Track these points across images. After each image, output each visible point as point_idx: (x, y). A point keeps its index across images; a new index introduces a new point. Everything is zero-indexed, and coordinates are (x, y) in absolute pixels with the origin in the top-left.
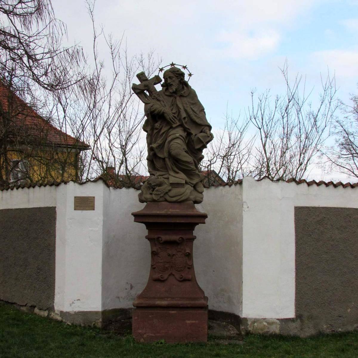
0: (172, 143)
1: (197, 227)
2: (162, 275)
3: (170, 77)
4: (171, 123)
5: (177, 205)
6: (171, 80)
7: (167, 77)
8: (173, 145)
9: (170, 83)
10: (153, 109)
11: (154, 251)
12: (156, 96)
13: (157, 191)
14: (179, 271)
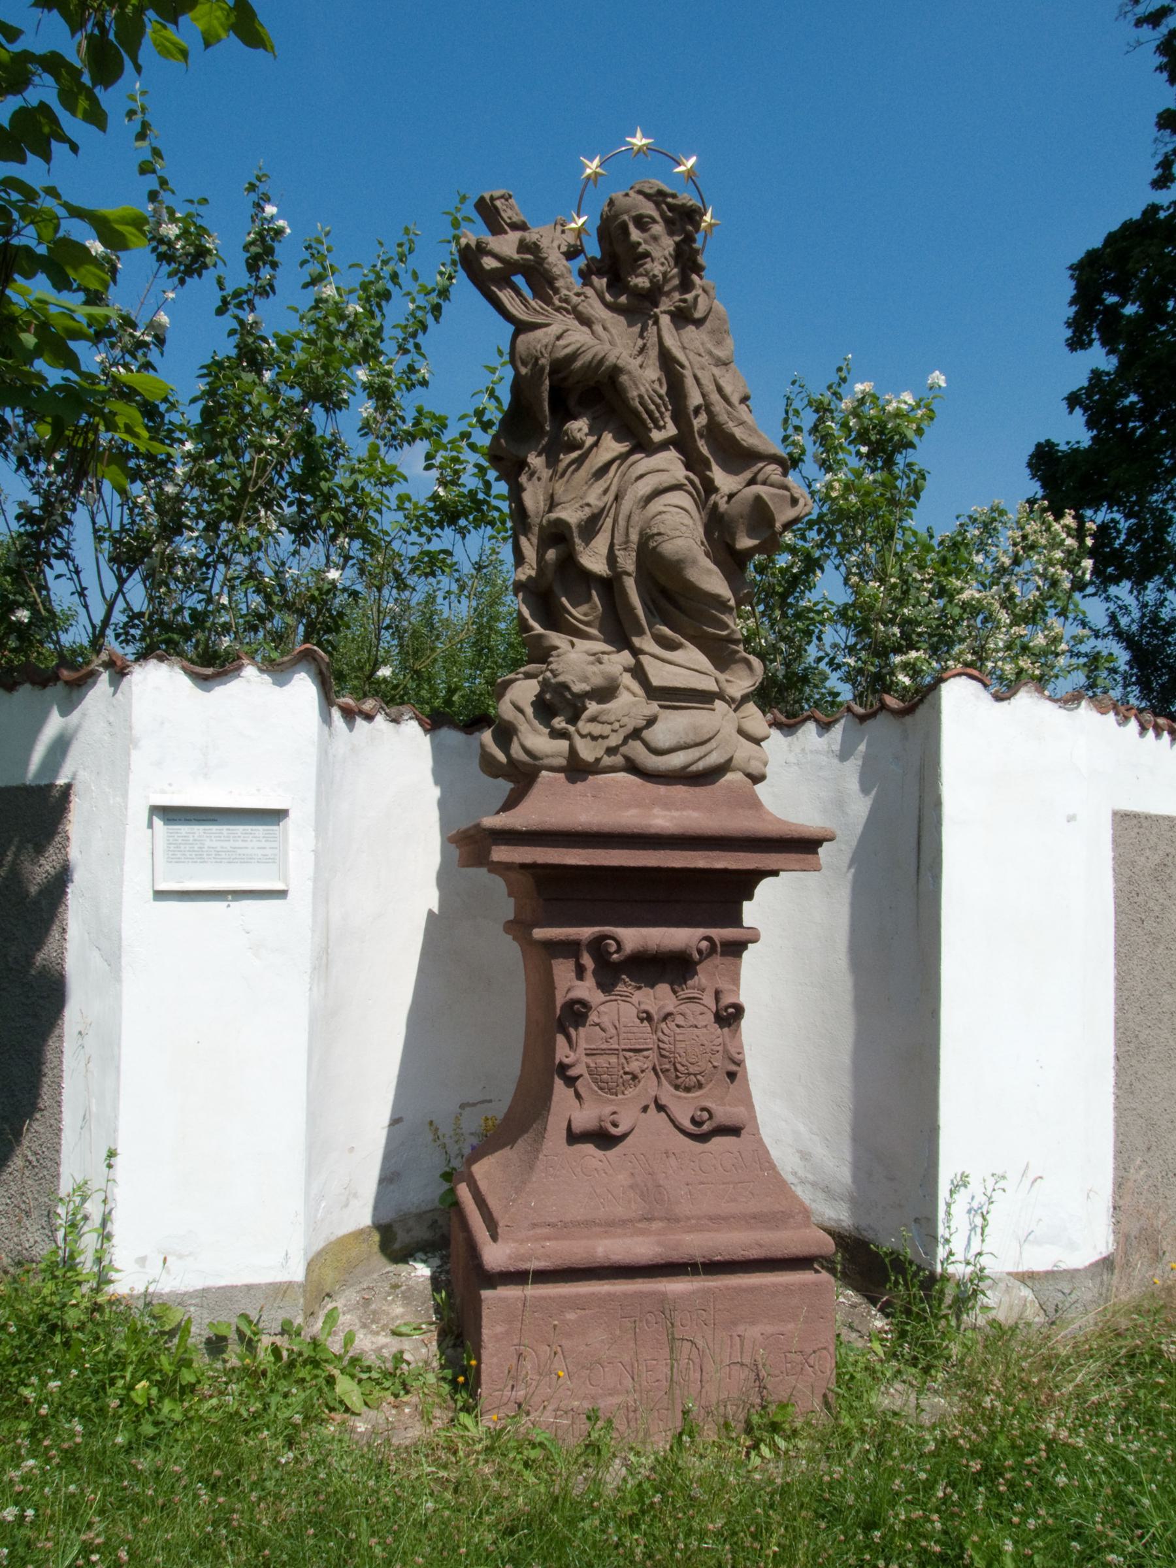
0: (657, 505)
1: (765, 889)
2: (614, 1113)
3: (642, 222)
5: (680, 791)
7: (626, 217)
8: (664, 516)
9: (639, 244)
10: (568, 350)
12: (575, 300)
14: (688, 1090)
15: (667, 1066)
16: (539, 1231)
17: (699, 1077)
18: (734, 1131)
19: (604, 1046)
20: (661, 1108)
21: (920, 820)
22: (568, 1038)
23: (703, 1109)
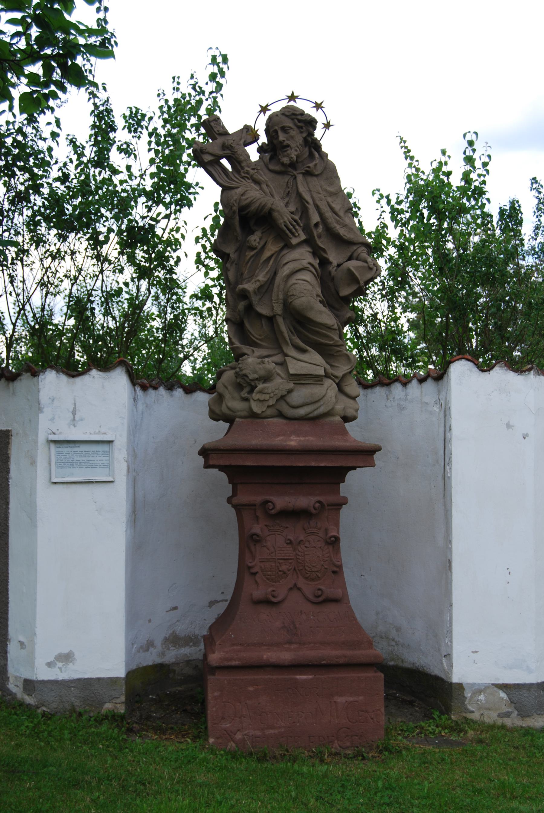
0: (292, 281)
1: (351, 476)
2: (273, 591)
3: (284, 129)
4: (287, 235)
6: (286, 135)
7: (276, 128)
8: (296, 286)
9: (284, 141)
10: (248, 201)
11: (255, 534)
12: (252, 172)
13: (261, 392)
14: (313, 580)
15: (301, 568)
16: (235, 647)
17: (317, 574)
18: (336, 601)
19: (268, 557)
20: (299, 589)
21: (445, 439)
22: (251, 552)
23: (319, 589)
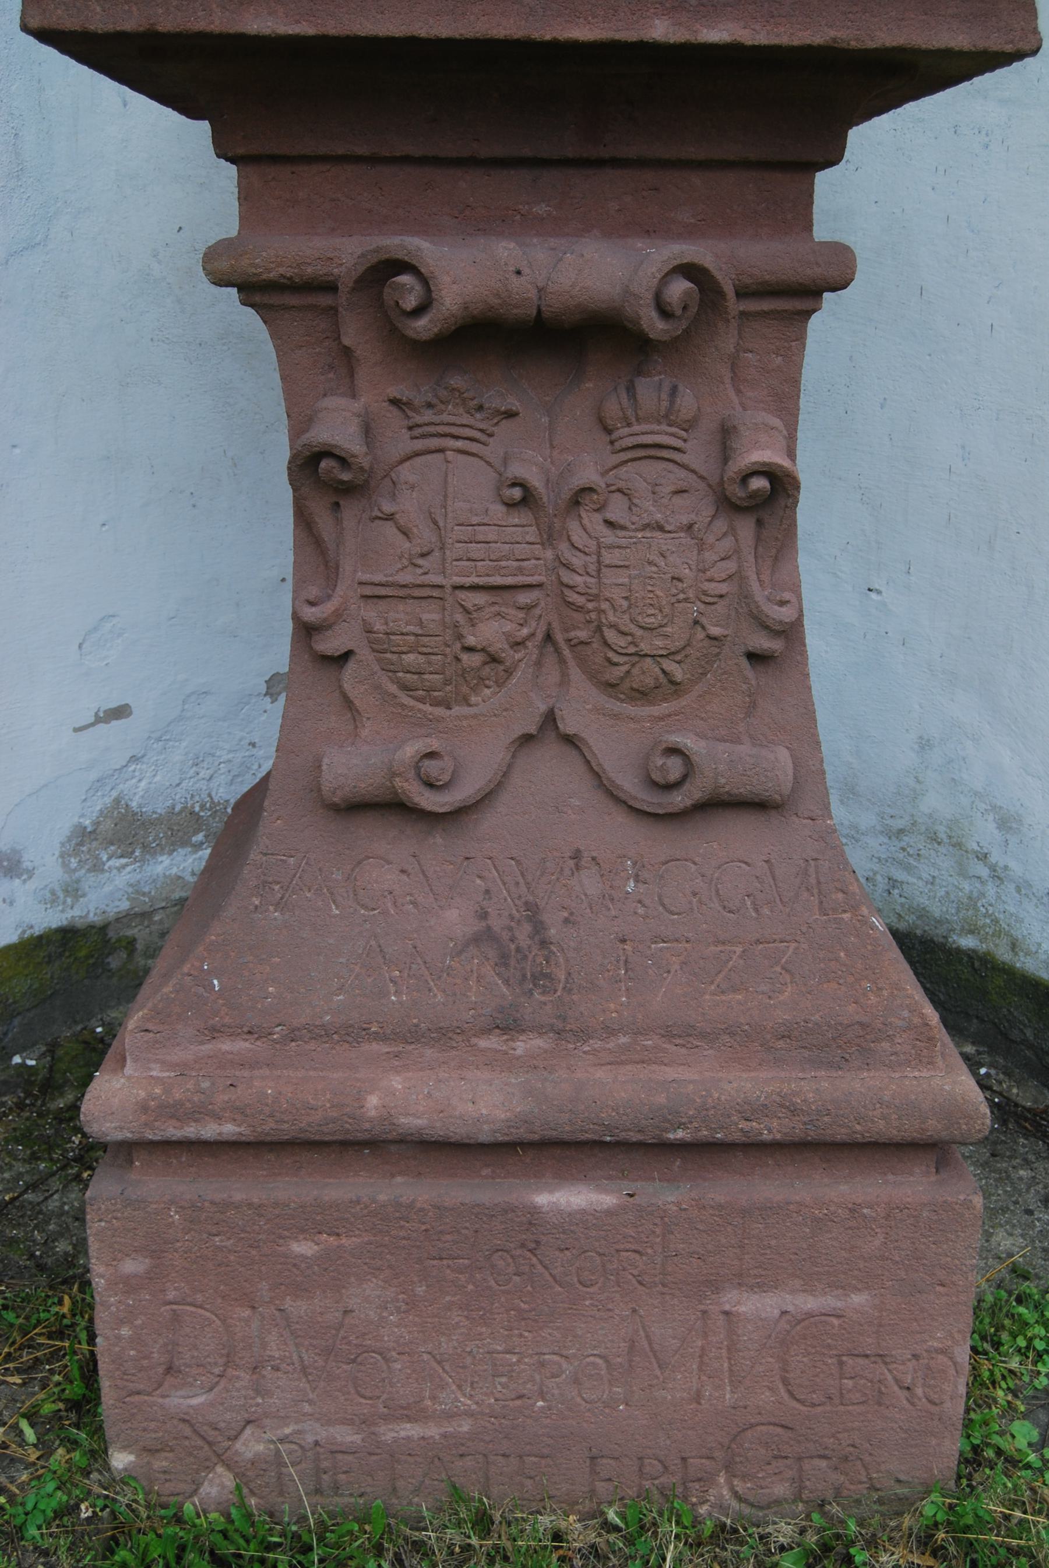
2: (432, 755)
11: (326, 453)
14: (642, 695)
15: (582, 634)
16: (226, 1046)
17: (669, 665)
19: (407, 577)
23: (673, 751)
